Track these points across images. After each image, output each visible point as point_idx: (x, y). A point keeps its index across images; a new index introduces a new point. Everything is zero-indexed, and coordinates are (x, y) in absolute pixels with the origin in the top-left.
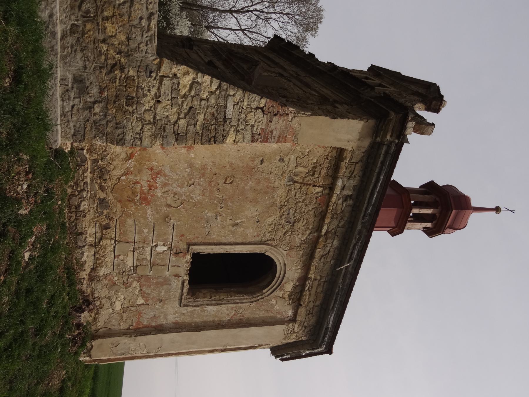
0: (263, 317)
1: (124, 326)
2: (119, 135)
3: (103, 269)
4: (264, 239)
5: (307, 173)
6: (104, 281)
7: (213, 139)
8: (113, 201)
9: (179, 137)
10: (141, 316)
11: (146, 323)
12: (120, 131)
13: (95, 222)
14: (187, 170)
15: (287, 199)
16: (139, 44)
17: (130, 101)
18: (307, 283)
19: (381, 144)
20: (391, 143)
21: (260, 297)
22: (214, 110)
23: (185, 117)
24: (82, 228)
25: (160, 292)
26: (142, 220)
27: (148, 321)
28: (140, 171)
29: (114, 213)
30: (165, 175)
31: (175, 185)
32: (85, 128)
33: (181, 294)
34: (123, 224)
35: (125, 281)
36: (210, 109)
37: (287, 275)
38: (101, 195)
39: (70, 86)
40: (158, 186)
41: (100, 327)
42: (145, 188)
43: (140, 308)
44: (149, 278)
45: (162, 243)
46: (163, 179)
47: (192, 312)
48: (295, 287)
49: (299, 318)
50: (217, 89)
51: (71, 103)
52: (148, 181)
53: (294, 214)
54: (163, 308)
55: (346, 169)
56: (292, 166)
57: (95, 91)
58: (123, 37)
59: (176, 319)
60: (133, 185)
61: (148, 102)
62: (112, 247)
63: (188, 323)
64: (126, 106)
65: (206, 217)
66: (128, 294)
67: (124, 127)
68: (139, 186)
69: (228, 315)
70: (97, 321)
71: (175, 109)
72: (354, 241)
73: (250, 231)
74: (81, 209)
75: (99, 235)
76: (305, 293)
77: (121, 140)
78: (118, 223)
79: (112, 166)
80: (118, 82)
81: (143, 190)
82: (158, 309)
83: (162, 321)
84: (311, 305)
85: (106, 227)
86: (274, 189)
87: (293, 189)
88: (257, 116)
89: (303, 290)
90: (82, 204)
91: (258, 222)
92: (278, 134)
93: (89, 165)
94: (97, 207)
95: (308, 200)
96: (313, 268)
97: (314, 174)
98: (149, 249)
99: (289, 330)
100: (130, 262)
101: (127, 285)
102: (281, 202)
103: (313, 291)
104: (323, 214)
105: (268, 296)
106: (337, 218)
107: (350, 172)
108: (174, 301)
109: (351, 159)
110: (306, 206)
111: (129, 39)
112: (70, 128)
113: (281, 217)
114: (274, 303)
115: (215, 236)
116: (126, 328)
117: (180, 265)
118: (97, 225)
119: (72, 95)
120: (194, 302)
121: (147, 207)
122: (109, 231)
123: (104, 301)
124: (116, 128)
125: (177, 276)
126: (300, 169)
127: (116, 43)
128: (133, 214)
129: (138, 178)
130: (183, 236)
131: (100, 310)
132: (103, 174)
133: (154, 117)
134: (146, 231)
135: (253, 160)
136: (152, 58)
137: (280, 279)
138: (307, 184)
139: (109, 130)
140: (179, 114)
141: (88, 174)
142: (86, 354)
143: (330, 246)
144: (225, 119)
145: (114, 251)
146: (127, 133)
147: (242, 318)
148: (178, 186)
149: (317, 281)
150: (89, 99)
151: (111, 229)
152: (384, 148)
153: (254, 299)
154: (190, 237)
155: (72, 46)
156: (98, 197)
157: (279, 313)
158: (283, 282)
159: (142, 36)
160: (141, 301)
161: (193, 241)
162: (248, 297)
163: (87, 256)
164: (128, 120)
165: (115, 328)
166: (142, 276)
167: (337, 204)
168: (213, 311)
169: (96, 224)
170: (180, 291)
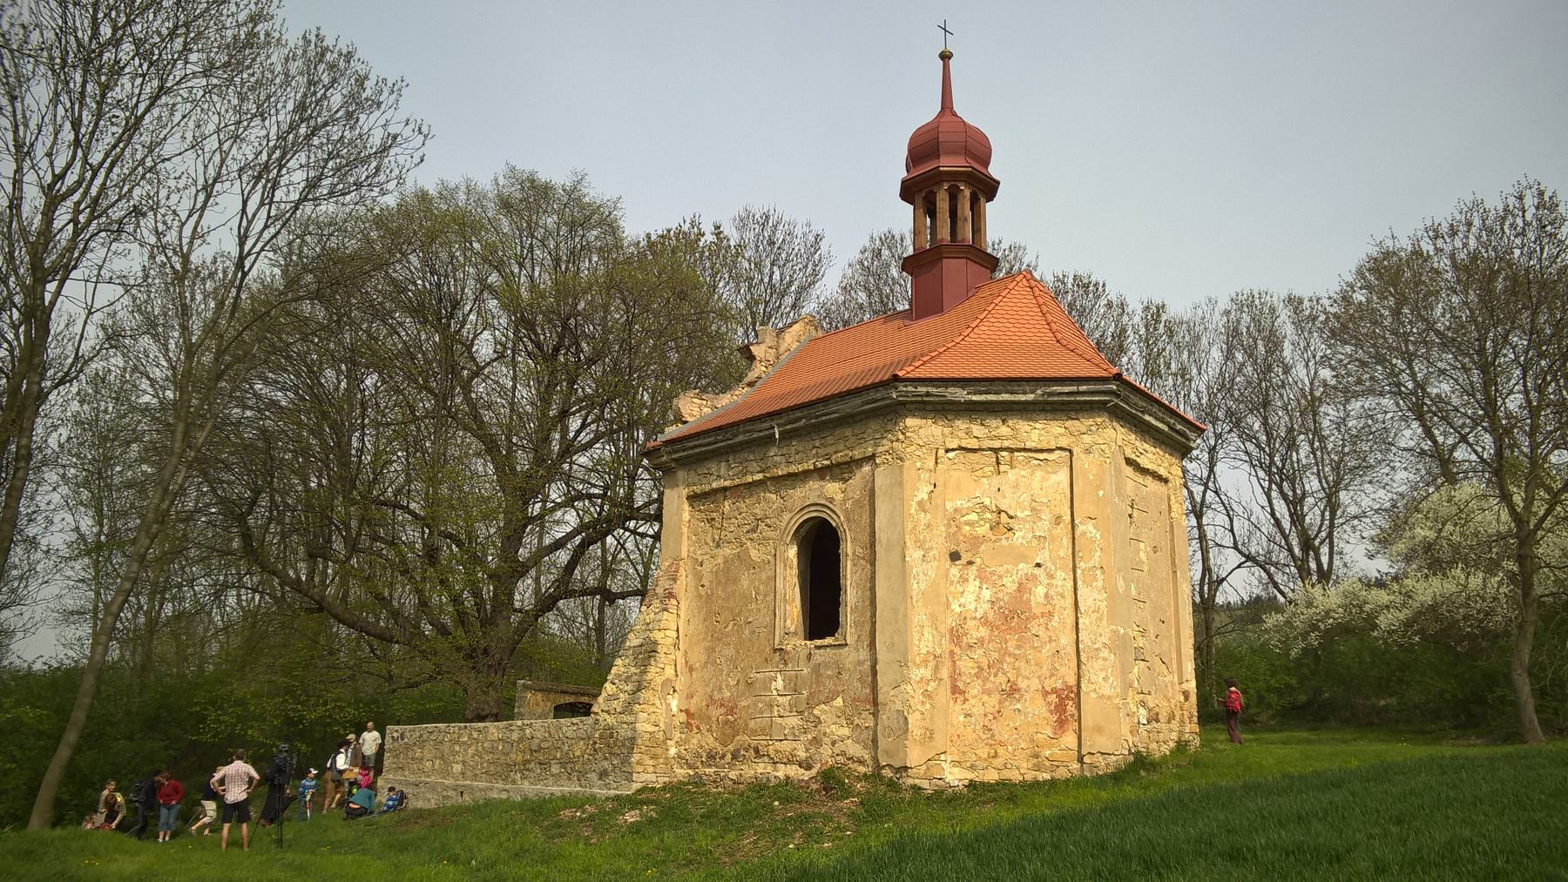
11: (868, 691)
19: (674, 460)
25: (829, 677)
26: (750, 711)
28: (709, 718)
30: (712, 692)
34: (754, 732)
38: (729, 756)
42: (723, 710)
46: (716, 692)
48: (834, 479)
57: (606, 763)
58: (582, 743)
61: (610, 720)
71: (622, 695)
85: (757, 750)
93: (701, 771)
95: (736, 514)
97: (714, 519)
98: (778, 698)
100: (794, 721)
101: (818, 721)
103: (830, 450)
108: (841, 655)
110: (740, 514)
114: (850, 502)
122: (760, 748)
129: (714, 719)
130: (766, 659)
135: (700, 596)
136: (589, 720)
141: (707, 770)
142: (904, 774)
144: (641, 646)
145: (781, 740)
149: (819, 450)
152: (674, 456)
153: (844, 537)
158: (823, 502)
163: (782, 772)
170: (828, 650)
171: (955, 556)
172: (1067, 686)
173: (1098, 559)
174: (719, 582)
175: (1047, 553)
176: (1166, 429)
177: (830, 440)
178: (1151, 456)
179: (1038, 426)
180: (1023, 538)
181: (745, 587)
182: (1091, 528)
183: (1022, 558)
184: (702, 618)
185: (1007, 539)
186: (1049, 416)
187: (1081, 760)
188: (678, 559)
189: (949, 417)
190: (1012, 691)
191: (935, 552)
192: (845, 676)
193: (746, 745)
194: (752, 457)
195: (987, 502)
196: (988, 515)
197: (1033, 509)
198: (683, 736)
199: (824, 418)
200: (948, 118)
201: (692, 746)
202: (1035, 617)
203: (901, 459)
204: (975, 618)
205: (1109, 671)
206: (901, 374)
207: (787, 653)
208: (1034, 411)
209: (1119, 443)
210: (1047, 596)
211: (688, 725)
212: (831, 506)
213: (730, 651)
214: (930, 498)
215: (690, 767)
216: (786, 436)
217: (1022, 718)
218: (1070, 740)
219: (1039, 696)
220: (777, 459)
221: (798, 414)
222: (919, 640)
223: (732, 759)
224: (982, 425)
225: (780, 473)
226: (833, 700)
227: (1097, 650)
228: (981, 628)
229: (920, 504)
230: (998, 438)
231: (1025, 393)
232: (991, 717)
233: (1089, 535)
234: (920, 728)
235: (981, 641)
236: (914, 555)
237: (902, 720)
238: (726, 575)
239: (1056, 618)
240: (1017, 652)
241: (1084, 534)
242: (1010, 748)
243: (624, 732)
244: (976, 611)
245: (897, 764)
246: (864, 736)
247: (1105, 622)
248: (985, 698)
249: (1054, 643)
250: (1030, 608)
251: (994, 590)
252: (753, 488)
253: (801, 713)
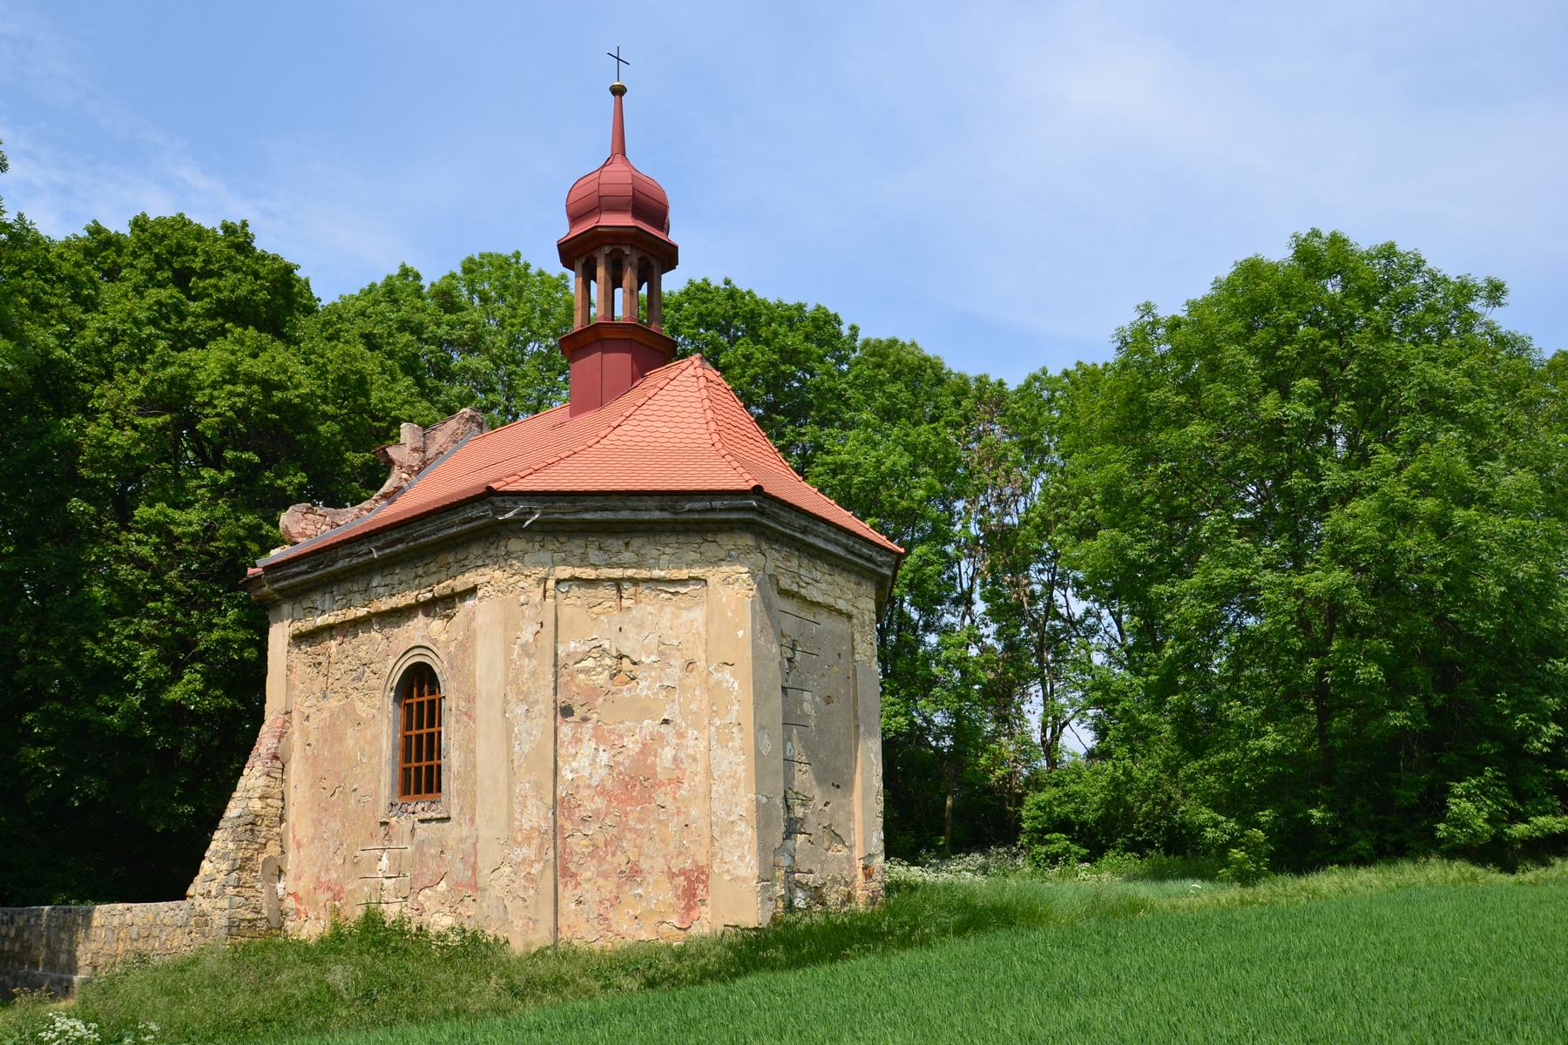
19: (277, 591)
98: (385, 881)
103: (434, 579)
129: (321, 904)
135: (307, 758)
171: (567, 711)
172: (697, 866)
173: (735, 714)
174: (326, 741)
175: (676, 707)
176: (842, 552)
177: (433, 567)
178: (824, 586)
179: (668, 550)
180: (649, 689)
182: (728, 676)
183: (645, 712)
185: (629, 689)
186: (682, 539)
189: (562, 540)
190: (633, 874)
191: (541, 706)
192: (448, 856)
194: (355, 588)
195: (606, 645)
196: (608, 661)
197: (661, 653)
200: (618, 165)
202: (661, 784)
204: (589, 786)
205: (746, 847)
206: (495, 486)
209: (770, 570)
210: (675, 759)
213: (336, 825)
214: (535, 640)
217: (644, 904)
219: (665, 878)
220: (380, 590)
221: (396, 535)
222: (522, 813)
224: (600, 548)
227: (732, 822)
228: (596, 798)
229: (524, 647)
230: (620, 565)
231: (648, 510)
232: (607, 904)
233: (725, 685)
234: (521, 918)
235: (595, 816)
237: (502, 908)
238: (332, 734)
239: (686, 785)
240: (639, 826)
241: (719, 683)
244: (591, 777)
247: (742, 790)
248: (601, 881)
249: (682, 817)
250: (655, 774)
251: (613, 752)
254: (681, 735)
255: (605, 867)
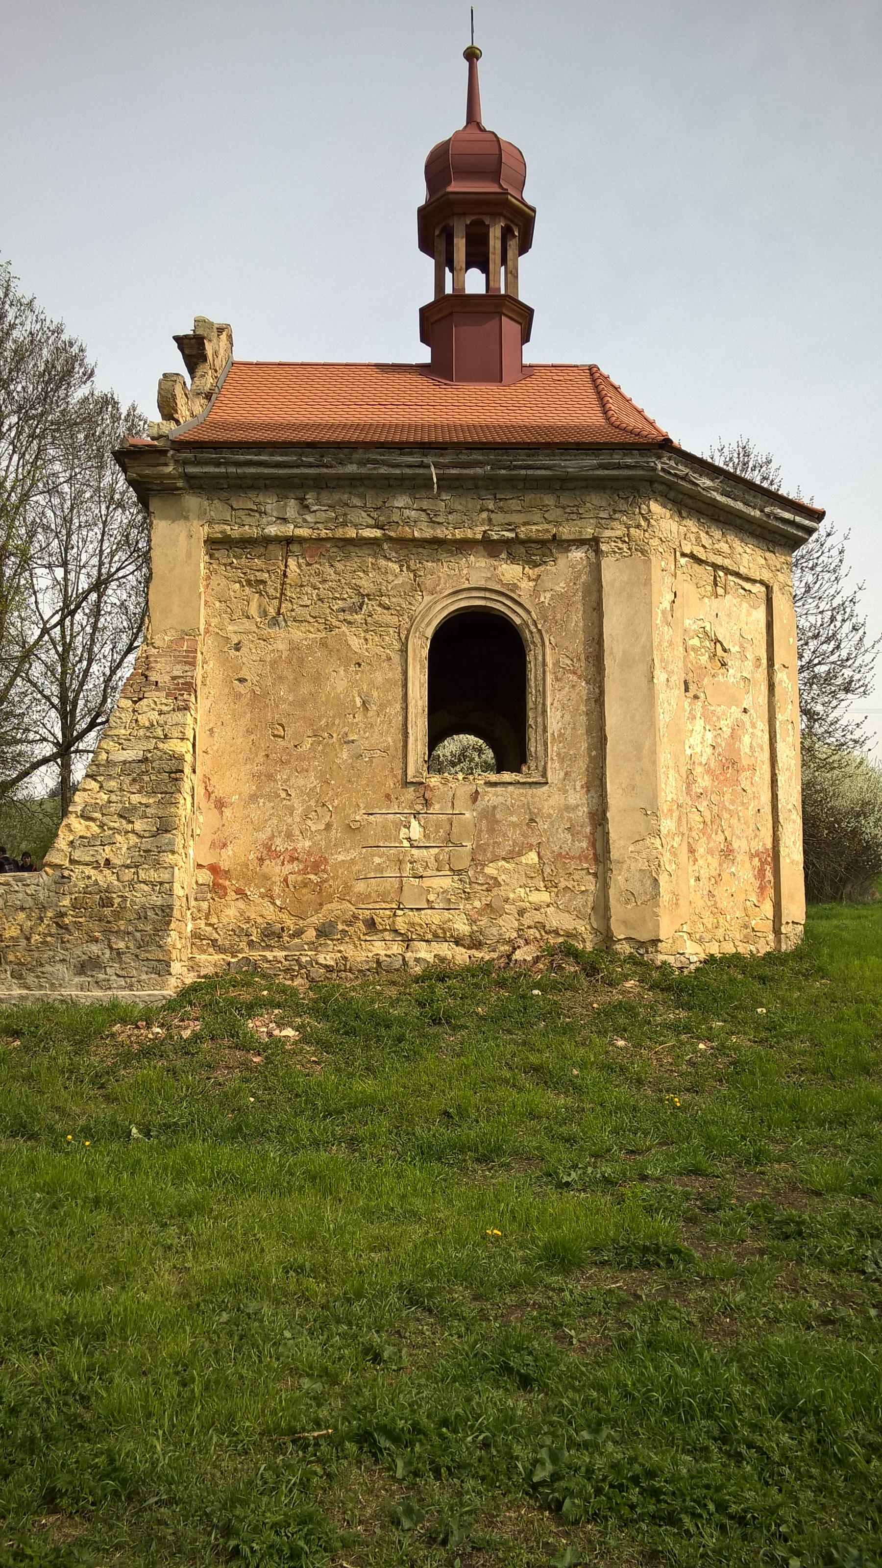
0: (584, 612)
1: (590, 885)
2: (157, 914)
3: (455, 926)
4: (397, 646)
5: (261, 594)
6: (481, 923)
7: (173, 775)
8: (320, 915)
9: (165, 827)
10: (567, 854)
11: (584, 845)
12: (150, 913)
13: (362, 943)
14: (261, 804)
15: (312, 620)
16: (28, 895)
17: (106, 902)
18: (496, 537)
19: (187, 477)
20: (177, 462)
21: (532, 628)
22: (127, 780)
23: (133, 823)
24: (367, 962)
25: (514, 825)
26: (355, 868)
27: (580, 841)
28: (266, 878)
29: (344, 913)
30: (272, 838)
31: (289, 821)
32: (148, 959)
33: (519, 786)
34: (364, 898)
35: (484, 888)
36: (125, 787)
37: (482, 583)
38: (311, 934)
39: (89, 979)
40: (290, 848)
41: (588, 927)
42: (296, 866)
43: (548, 855)
44: (479, 846)
45: (404, 830)
46: (278, 841)
47: (562, 759)
48: (513, 558)
49: (589, 532)
50: (95, 780)
51: (114, 977)
52: (283, 864)
53: (345, 599)
54: (550, 816)
55: (244, 525)
56: (248, 625)
57: (95, 949)
58: (22, 916)
59: (578, 788)
60: (291, 886)
61: (105, 878)
62: (411, 913)
63: (590, 762)
64: (113, 906)
65: (350, 761)
66: (515, 881)
67: (143, 907)
68: (291, 878)
69: (573, 686)
70: (574, 932)
71: (119, 838)
72: (383, 470)
73: (379, 678)
74: (332, 963)
75: (387, 935)
76: (522, 536)
77: (163, 911)
78: (363, 907)
79: (260, 920)
80: (80, 920)
81: (299, 870)
82: (552, 824)
83: (583, 812)
84: (555, 514)
85: (371, 924)
86: (294, 648)
87: (293, 613)
88: (145, 709)
89: (517, 541)
90: (324, 962)
91: (360, 665)
92: (178, 667)
93: (255, 955)
94: (332, 940)
95: (315, 580)
96: (459, 534)
98: (415, 851)
99: (619, 549)
100: (446, 882)
102: (319, 631)
103: (515, 518)
104: (340, 544)
105: (529, 612)
106: (345, 515)
107: (249, 515)
109: (225, 522)
110: (325, 581)
111: (22, 909)
112: (149, 979)
113: (350, 623)
114: (548, 595)
115: (390, 739)
116: (593, 880)
117: (451, 794)
118: (368, 938)
119: (102, 976)
120: (537, 758)
121: (331, 862)
122: (378, 920)
123: (527, 921)
124: (146, 918)
125: (475, 797)
126: (253, 611)
127: (29, 923)
128: (345, 883)
131: (547, 928)
132: (273, 933)
133: (128, 867)
134: (377, 860)
136: (45, 877)
137: (488, 595)
138: (282, 589)
139: (149, 928)
140: (127, 832)
141: (269, 955)
142: (650, 949)
143: (407, 512)
144: (145, 760)
146: (152, 902)
147: (583, 657)
148: (291, 814)
149: (493, 516)
150: (107, 956)
151: (375, 917)
152: (190, 470)
153: (537, 639)
154: (390, 783)
155: (38, 977)
156: (314, 939)
157: (577, 578)
158: (498, 587)
159: (16, 892)
160: (532, 857)
161: (399, 777)
162: (532, 652)
163: (425, 952)
164: (133, 903)
165: (591, 899)
166: (473, 860)
167: (316, 523)
168: (562, 717)
169: (366, 941)
170: (511, 788)
177: (514, 504)
181: (340, 689)
183: (734, 701)
184: (242, 729)
187: (777, 932)
188: (190, 634)
190: (727, 853)
192: (543, 825)
193: (348, 916)
194: (356, 501)
195: (708, 628)
196: (707, 643)
198: (205, 905)
199: (523, 472)
201: (225, 920)
203: (643, 552)
207: (428, 788)
208: (746, 531)
211: (217, 889)
212: (516, 597)
213: (312, 781)
214: (672, 609)
215: (221, 950)
216: (448, 484)
218: (768, 909)
221: (477, 456)
223: (318, 937)
225: (417, 534)
226: (520, 854)
227: (790, 811)
228: (705, 776)
229: (664, 612)
230: (719, 553)
233: (784, 685)
236: (660, 677)
237: (648, 883)
239: (758, 773)
242: (728, 917)
243: (142, 896)
245: (644, 937)
246: (579, 901)
249: (756, 801)
252: (352, 548)
253: (459, 872)
254: (754, 726)
255: (711, 845)
